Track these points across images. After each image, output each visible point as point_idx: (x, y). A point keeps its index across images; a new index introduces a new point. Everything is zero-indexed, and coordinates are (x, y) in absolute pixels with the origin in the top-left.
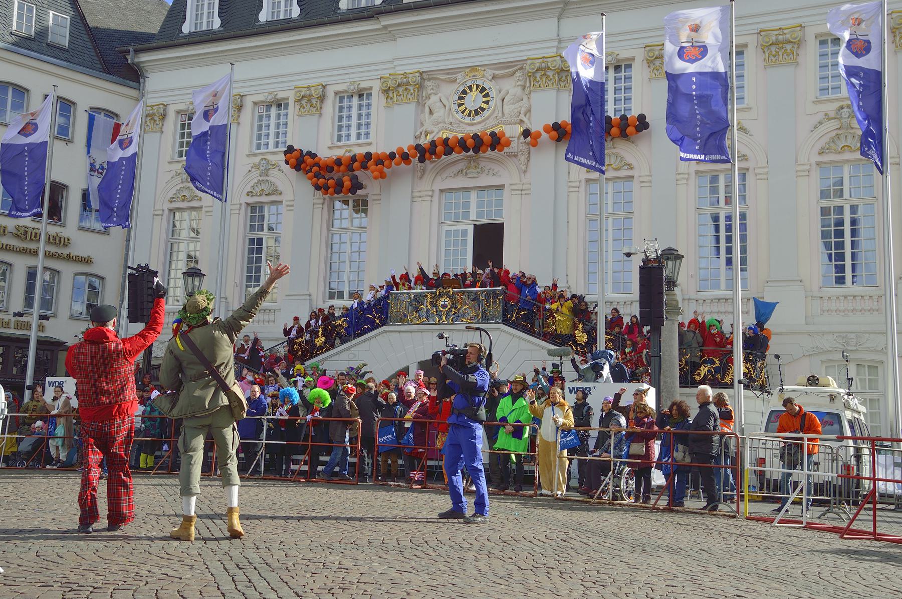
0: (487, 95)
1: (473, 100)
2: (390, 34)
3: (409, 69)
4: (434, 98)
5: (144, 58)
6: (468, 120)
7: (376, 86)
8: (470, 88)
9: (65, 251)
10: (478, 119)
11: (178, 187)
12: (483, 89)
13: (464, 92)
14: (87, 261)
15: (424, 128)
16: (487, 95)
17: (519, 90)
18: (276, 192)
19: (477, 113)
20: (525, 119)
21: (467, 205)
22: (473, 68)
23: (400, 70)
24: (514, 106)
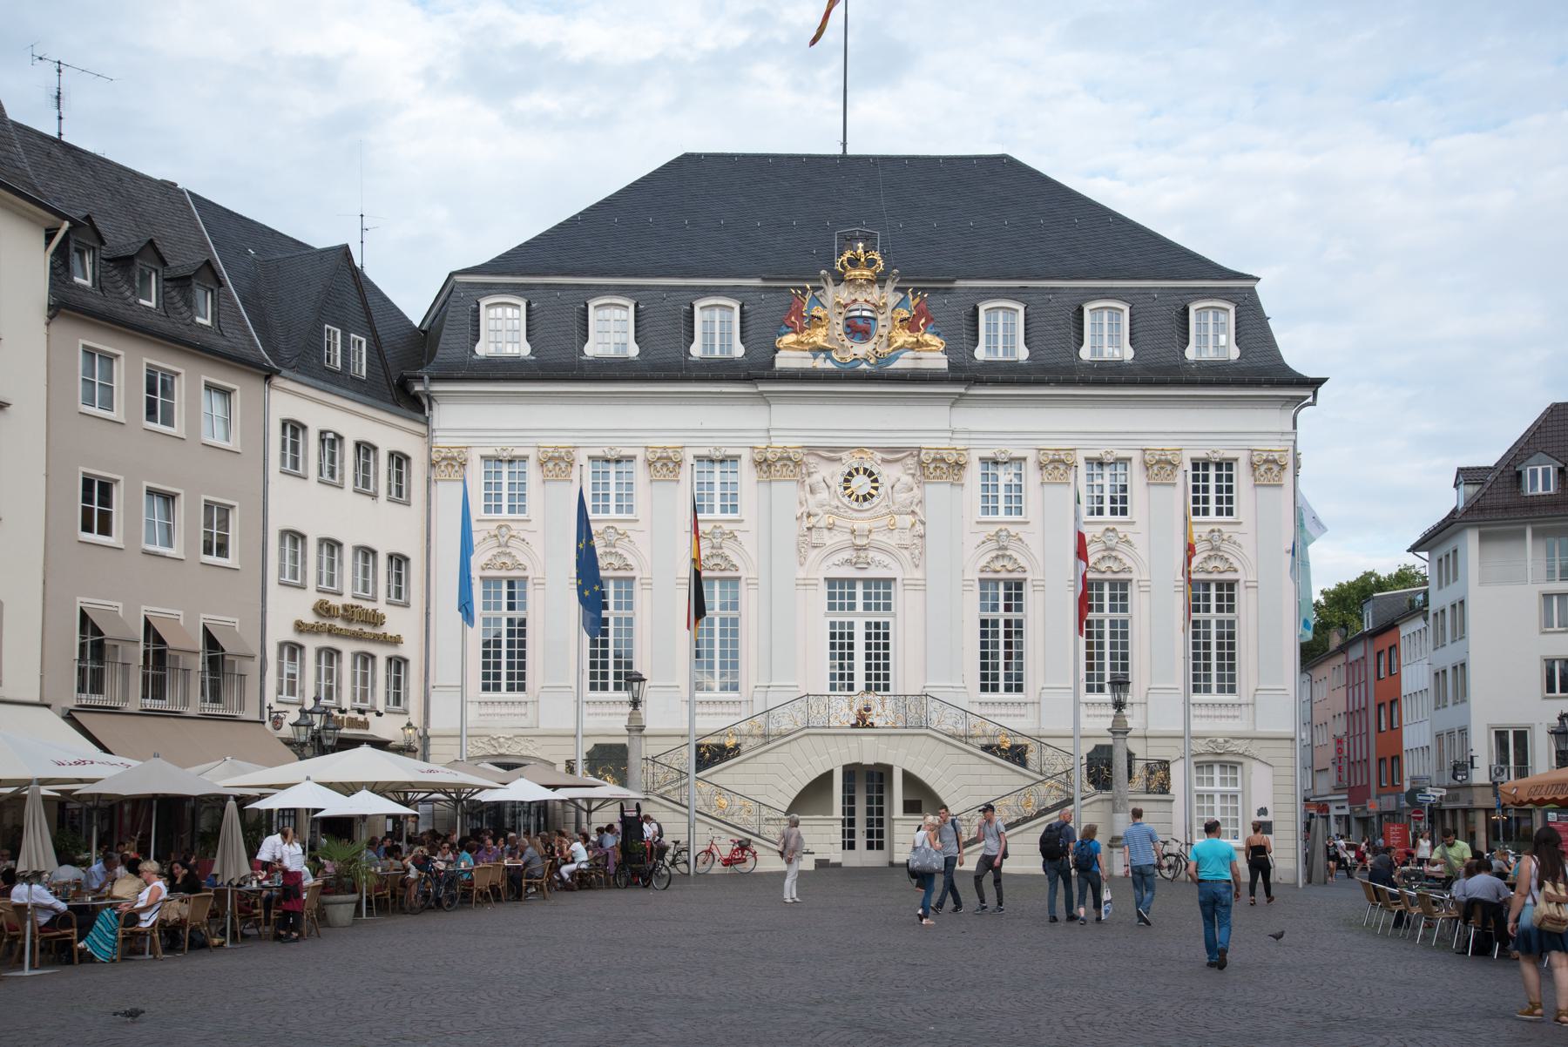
0: (876, 481)
1: (861, 484)
2: (765, 399)
3: (792, 443)
4: (816, 478)
5: (437, 387)
6: (855, 506)
7: (746, 455)
8: (857, 470)
9: (380, 631)
10: (866, 505)
11: (495, 551)
12: (871, 474)
13: (850, 474)
14: (396, 641)
15: (804, 509)
16: (876, 481)
17: (909, 479)
18: (628, 567)
19: (865, 499)
20: (917, 510)
21: (852, 596)
22: (860, 449)
23: (778, 443)
24: (904, 495)
